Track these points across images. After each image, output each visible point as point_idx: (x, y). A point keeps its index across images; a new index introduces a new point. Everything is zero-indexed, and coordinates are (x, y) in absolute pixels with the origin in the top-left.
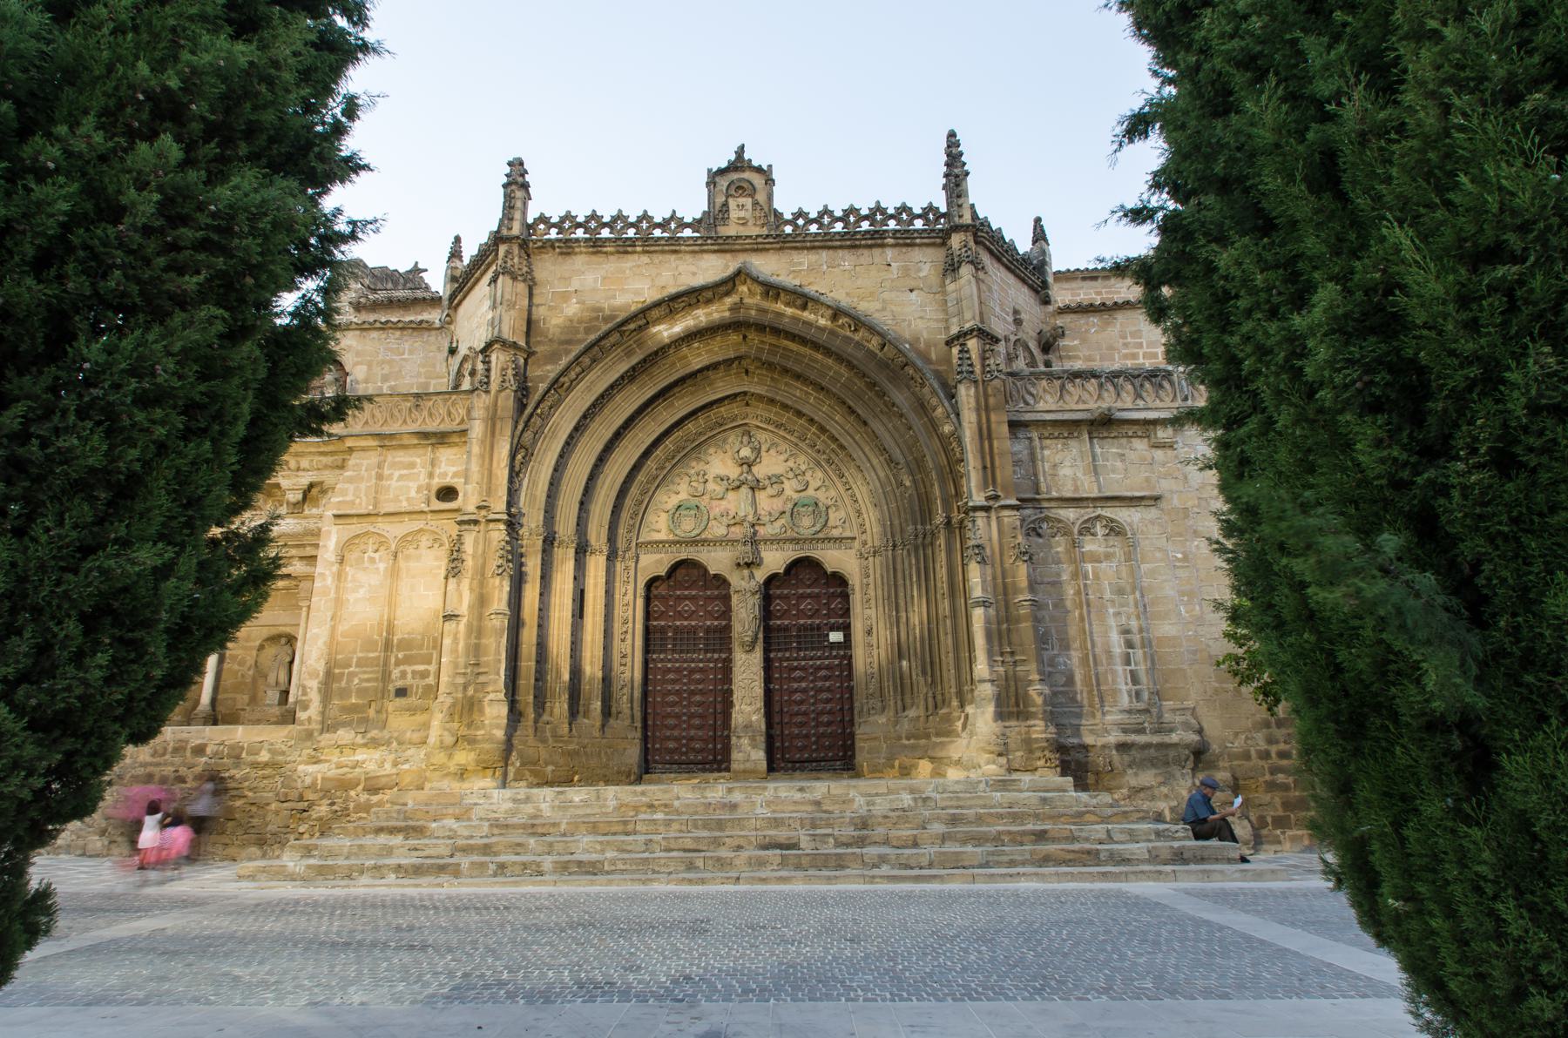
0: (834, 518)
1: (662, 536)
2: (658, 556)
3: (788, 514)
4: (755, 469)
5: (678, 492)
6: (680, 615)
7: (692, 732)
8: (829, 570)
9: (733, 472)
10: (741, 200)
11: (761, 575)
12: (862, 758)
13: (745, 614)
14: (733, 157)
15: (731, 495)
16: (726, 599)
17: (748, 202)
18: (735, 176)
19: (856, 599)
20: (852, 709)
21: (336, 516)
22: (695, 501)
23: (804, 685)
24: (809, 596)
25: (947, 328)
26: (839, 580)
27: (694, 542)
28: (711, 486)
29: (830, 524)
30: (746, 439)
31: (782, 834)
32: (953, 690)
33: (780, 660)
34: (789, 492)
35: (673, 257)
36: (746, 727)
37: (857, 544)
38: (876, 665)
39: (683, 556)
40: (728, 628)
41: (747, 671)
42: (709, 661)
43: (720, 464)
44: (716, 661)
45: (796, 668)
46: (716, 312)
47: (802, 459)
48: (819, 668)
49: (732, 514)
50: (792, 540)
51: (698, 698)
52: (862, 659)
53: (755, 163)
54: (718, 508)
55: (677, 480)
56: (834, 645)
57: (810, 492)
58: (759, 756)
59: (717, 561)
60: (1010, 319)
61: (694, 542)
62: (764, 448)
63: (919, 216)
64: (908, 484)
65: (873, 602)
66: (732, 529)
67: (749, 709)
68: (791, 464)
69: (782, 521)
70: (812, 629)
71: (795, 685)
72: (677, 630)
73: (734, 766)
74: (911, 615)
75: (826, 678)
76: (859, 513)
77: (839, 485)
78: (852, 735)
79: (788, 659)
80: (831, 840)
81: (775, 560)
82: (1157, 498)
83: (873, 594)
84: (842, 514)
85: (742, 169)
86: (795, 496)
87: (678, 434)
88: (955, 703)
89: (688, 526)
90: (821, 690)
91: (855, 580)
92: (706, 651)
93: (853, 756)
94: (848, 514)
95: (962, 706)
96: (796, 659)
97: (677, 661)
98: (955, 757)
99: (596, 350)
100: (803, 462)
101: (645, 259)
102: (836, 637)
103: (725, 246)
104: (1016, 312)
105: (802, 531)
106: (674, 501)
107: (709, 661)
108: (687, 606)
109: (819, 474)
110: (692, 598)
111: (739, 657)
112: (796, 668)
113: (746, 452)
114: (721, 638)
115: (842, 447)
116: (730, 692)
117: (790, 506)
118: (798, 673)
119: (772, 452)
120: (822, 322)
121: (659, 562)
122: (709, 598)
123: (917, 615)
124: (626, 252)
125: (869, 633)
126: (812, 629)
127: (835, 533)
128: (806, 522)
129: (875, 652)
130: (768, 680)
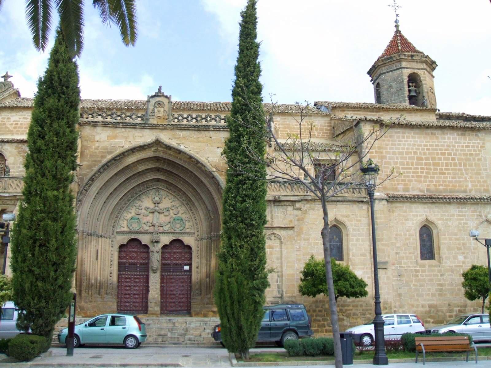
0: (188, 224)
1: (125, 229)
4: (160, 205)
5: (131, 213)
6: (131, 258)
8: (185, 244)
10: (160, 109)
11: (160, 246)
12: (192, 311)
13: (156, 259)
14: (157, 91)
15: (151, 215)
16: (148, 253)
17: (162, 109)
18: (158, 99)
22: (137, 216)
24: (178, 253)
27: (137, 232)
29: (187, 227)
31: (163, 332)
33: (167, 276)
34: (172, 214)
35: (133, 130)
38: (199, 279)
40: (147, 264)
41: (155, 281)
42: (141, 275)
43: (147, 202)
44: (143, 275)
45: (172, 279)
46: (148, 154)
49: (151, 222)
50: (172, 233)
51: (137, 288)
52: (195, 277)
53: (165, 94)
54: (145, 220)
55: (131, 208)
56: (186, 271)
57: (180, 215)
58: (158, 309)
59: (145, 239)
61: (137, 232)
62: (164, 197)
64: (212, 217)
69: (169, 226)
70: (178, 265)
72: (130, 264)
73: (149, 312)
76: (197, 224)
77: (191, 213)
78: (190, 302)
79: (169, 275)
81: (166, 240)
82: (293, 228)
84: (191, 224)
85: (160, 96)
89: (135, 226)
90: (180, 286)
91: (194, 248)
92: (140, 272)
93: (190, 310)
99: (106, 167)
100: (177, 203)
101: (123, 130)
102: (187, 268)
103: (153, 127)
105: (176, 229)
107: (141, 275)
109: (184, 208)
110: (135, 252)
112: (172, 279)
113: (157, 199)
114: (146, 267)
117: (172, 220)
118: (173, 280)
119: (167, 198)
121: (124, 239)
122: (141, 252)
124: (117, 127)
126: (178, 265)
127: (188, 231)
128: (178, 226)
129: (199, 274)
130: (162, 282)
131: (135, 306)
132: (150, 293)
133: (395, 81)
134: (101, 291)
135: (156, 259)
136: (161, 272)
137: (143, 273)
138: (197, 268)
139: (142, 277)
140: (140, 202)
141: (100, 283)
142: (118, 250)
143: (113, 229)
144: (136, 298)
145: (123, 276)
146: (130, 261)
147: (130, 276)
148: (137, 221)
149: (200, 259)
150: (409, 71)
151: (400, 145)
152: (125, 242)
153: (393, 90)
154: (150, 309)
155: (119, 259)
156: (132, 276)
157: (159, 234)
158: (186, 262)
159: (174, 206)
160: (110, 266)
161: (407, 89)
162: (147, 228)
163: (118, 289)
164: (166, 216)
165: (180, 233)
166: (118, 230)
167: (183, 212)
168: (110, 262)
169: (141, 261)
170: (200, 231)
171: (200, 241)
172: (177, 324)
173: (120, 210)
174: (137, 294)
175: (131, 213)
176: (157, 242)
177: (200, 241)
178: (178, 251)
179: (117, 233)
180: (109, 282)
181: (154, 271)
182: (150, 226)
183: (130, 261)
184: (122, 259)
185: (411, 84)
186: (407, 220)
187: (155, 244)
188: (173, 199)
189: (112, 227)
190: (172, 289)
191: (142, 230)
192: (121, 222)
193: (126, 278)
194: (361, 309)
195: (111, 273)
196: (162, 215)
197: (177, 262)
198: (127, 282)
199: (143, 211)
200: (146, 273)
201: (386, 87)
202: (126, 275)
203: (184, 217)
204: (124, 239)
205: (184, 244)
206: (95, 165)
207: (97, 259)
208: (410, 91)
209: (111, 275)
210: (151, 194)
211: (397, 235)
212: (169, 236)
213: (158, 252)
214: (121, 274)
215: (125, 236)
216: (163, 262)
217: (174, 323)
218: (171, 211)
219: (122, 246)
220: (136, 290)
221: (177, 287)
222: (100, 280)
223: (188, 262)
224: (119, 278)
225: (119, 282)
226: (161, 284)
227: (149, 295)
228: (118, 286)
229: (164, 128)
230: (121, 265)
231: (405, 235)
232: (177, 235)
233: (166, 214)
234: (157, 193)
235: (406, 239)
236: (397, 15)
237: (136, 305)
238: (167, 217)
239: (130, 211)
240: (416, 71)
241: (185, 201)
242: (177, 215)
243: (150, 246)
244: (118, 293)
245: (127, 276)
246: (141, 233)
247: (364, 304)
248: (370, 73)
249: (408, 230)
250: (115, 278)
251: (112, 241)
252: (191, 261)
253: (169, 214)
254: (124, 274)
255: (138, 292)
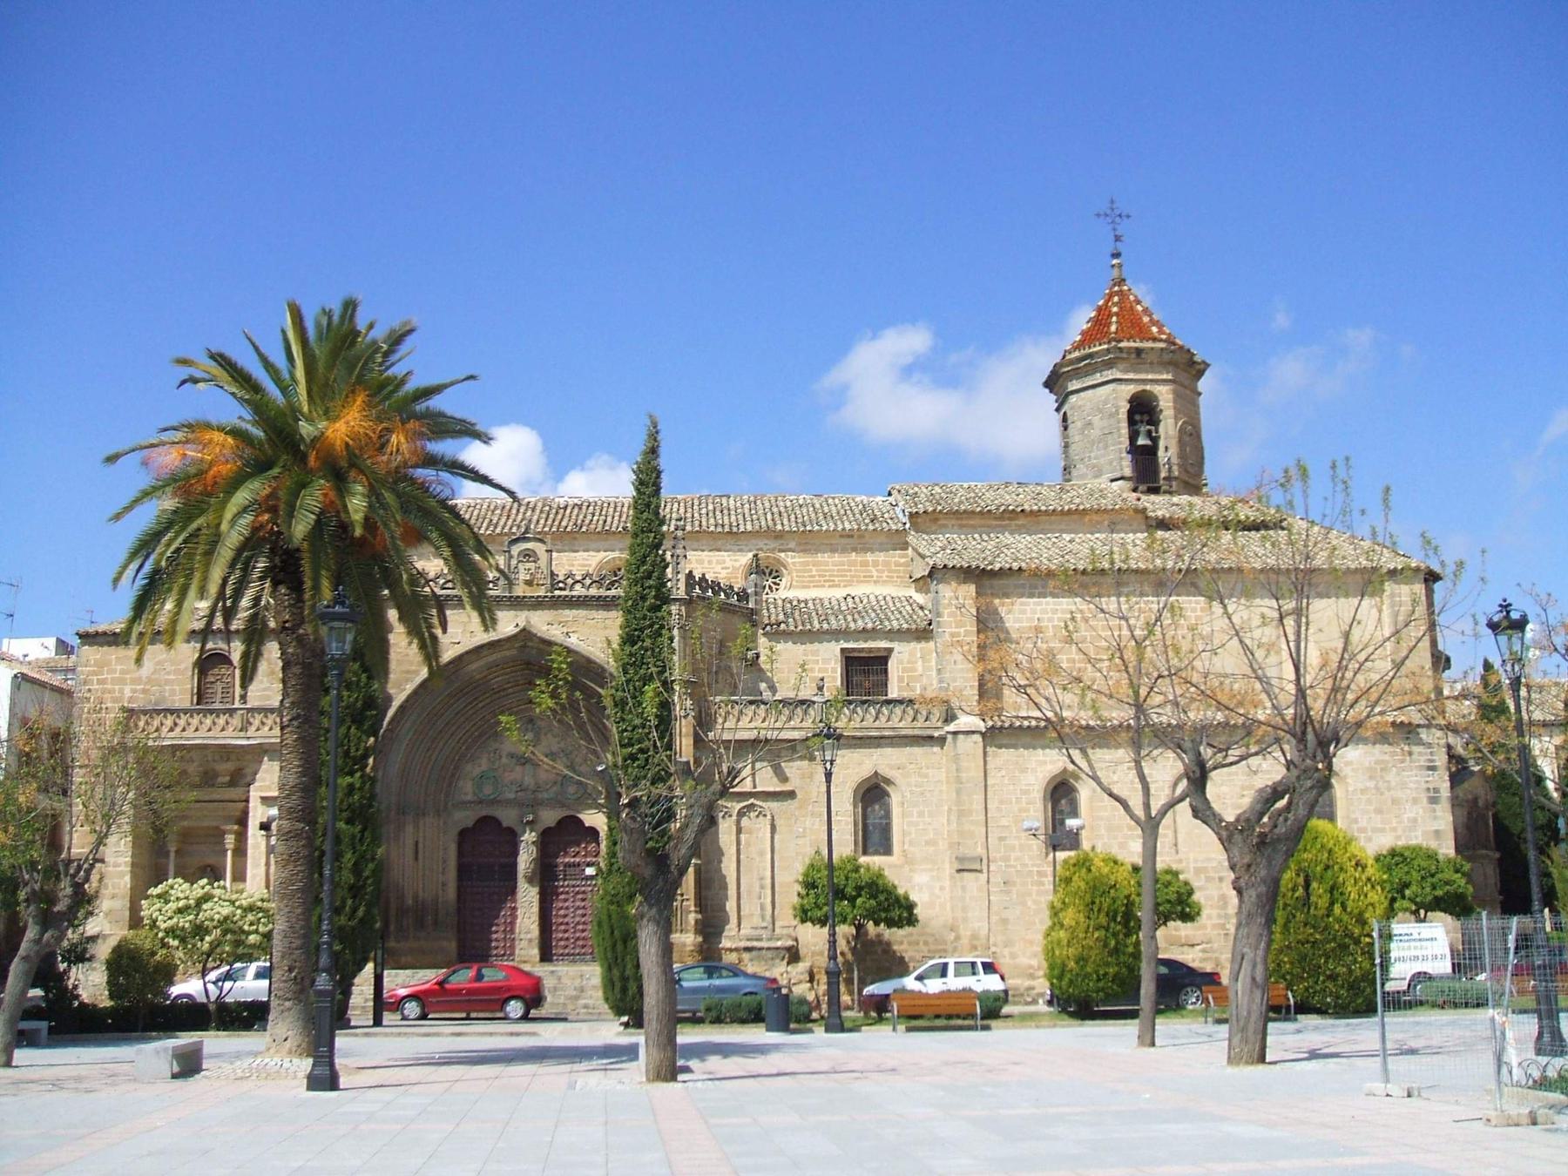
1: (469, 797)
15: (518, 768)
21: (263, 798)
28: (504, 760)
39: (484, 813)
59: (508, 817)
61: (494, 802)
89: (488, 790)
106: (477, 771)
133: (1100, 411)
150: (1131, 389)
151: (1024, 612)
152: (470, 823)
153: (1095, 433)
161: (1125, 431)
172: (564, 980)
185: (1137, 417)
186: (1024, 770)
192: (461, 783)
194: (925, 949)
201: (1079, 424)
204: (466, 818)
206: (407, 681)
207: (416, 858)
208: (1133, 437)
211: (1001, 802)
217: (559, 978)
219: (463, 834)
228: (459, 910)
229: (538, 604)
230: (463, 870)
231: (1018, 800)
235: (1020, 811)
236: (1118, 239)
240: (1148, 387)
247: (931, 940)
248: (1047, 384)
249: (1026, 792)
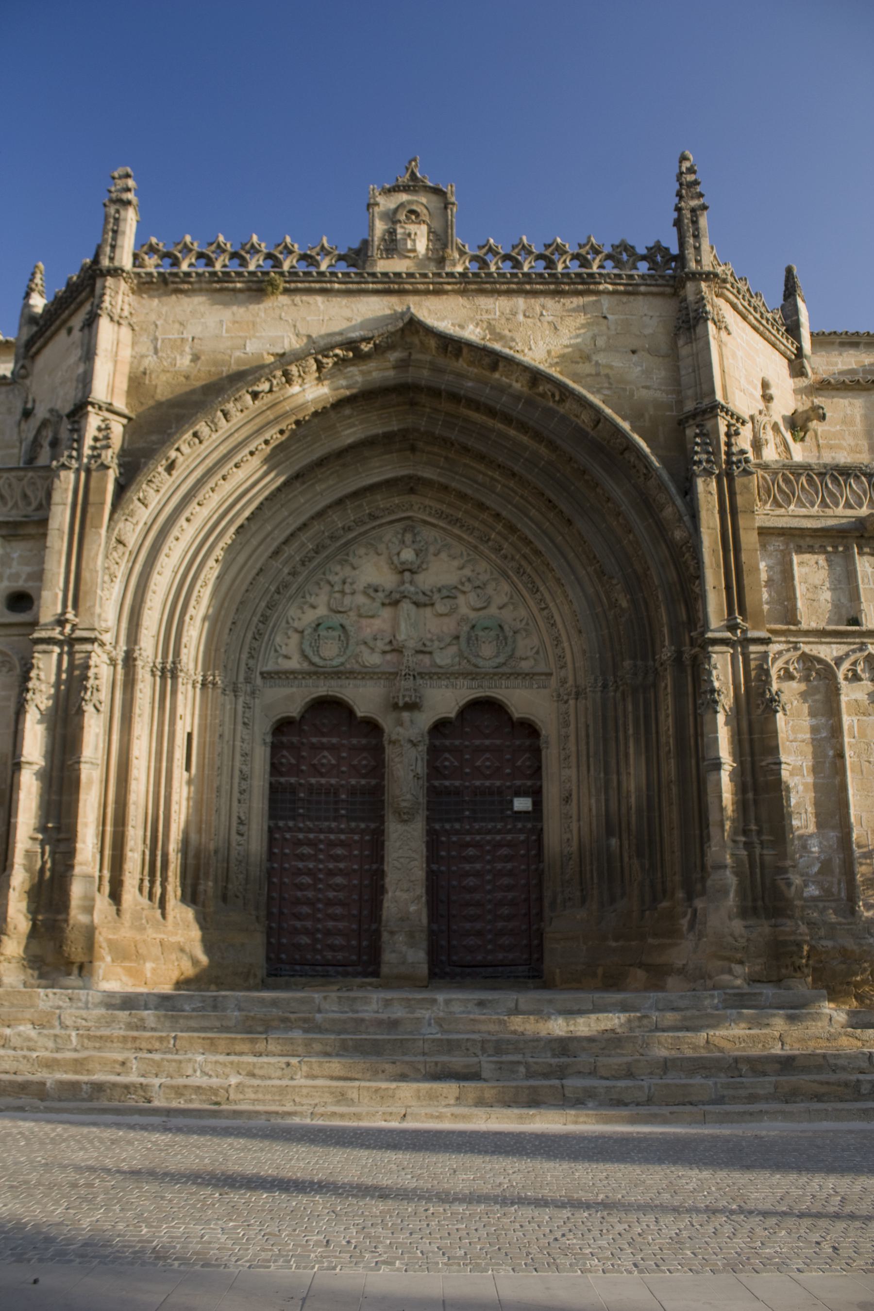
0: (525, 645)
1: (294, 664)
2: (287, 691)
3: (463, 640)
4: (420, 578)
6: (316, 770)
7: (330, 924)
8: (516, 715)
9: (387, 579)
13: (406, 771)
15: (386, 613)
16: (378, 751)
19: (551, 756)
20: (540, 899)
22: (338, 619)
23: (478, 866)
25: (680, 403)
26: (529, 729)
27: (337, 674)
29: (519, 653)
30: (408, 537)
32: (678, 878)
34: (464, 610)
35: (319, 299)
36: (402, 919)
37: (553, 681)
38: (575, 843)
41: (405, 850)
42: (352, 831)
43: (373, 571)
45: (468, 845)
47: (483, 566)
48: (499, 845)
50: (465, 675)
57: (493, 610)
58: (417, 957)
60: (759, 392)
61: (337, 674)
62: (432, 549)
63: (644, 258)
64: (625, 604)
65: (573, 759)
66: (389, 657)
67: (405, 896)
68: (467, 572)
71: (467, 867)
72: (311, 789)
73: (385, 970)
74: (624, 778)
75: (509, 858)
76: (557, 641)
77: (531, 603)
78: (540, 934)
79: (457, 832)
80: (522, 1069)
81: (445, 700)
83: (573, 749)
86: (473, 615)
87: (317, 527)
88: (680, 895)
89: (330, 651)
93: (541, 960)
94: (543, 642)
95: (690, 897)
96: (468, 832)
97: (310, 830)
98: (679, 963)
102: (522, 804)
104: (765, 385)
105: (481, 663)
106: (310, 616)
107: (352, 831)
108: (328, 758)
109: (506, 587)
110: (332, 748)
111: (394, 830)
112: (468, 845)
113: (408, 555)
114: (372, 802)
115: (537, 553)
116: (380, 874)
117: (466, 628)
118: (471, 851)
119: (443, 555)
120: (517, 386)
123: (634, 779)
125: (567, 800)
127: (525, 666)
128: (487, 650)
129: (574, 826)
131: (332, 948)
132: (390, 895)
134: (201, 888)
135: (406, 771)
136: (429, 819)
137: (363, 826)
138: (567, 800)
139: (356, 837)
140: (348, 569)
141: (197, 856)
142: (269, 739)
143: (251, 662)
144: (334, 918)
145: (288, 836)
146: (313, 781)
147: (311, 836)
148: (336, 634)
149: (574, 770)
152: (294, 711)
154: (388, 957)
155: (272, 774)
156: (322, 836)
157: (420, 681)
158: (518, 783)
159: (469, 580)
160: (236, 795)
162: (373, 659)
163: (270, 883)
164: (441, 615)
165: (495, 674)
166: (265, 669)
167: (505, 599)
168: (236, 780)
169: (353, 782)
170: (570, 665)
171: (572, 702)
173: (276, 597)
174: (341, 903)
175: (314, 607)
176: (413, 707)
177: (572, 702)
178: (487, 742)
179: (266, 676)
180: (234, 854)
181: (405, 817)
182: (384, 652)
183: (313, 781)
184: (282, 774)
187: (406, 715)
188: (465, 558)
189: (244, 656)
190: (471, 881)
191: (356, 667)
193: (299, 843)
195: (241, 822)
196: (428, 611)
197: (487, 783)
198: (302, 857)
199: (361, 599)
200: (373, 826)
202: (300, 830)
203: (507, 615)
204: (292, 700)
205: (510, 718)
209: (243, 829)
210: (386, 539)
212: (454, 686)
213: (415, 745)
214: (279, 828)
215: (294, 689)
216: (436, 783)
218: (461, 599)
219: (283, 726)
220: (337, 888)
221: (489, 877)
222: (200, 844)
223: (529, 783)
224: (271, 841)
225: (271, 854)
226: (428, 865)
227: (386, 904)
228: (270, 872)
232: (486, 683)
233: (440, 608)
234: (408, 537)
237: (339, 941)
238: (446, 620)
239: (312, 600)
241: (513, 558)
242: (481, 613)
243: (380, 720)
244: (270, 898)
245: (301, 836)
246: (351, 674)
250: (256, 842)
251: (247, 706)
252: (540, 778)
253: (454, 610)
254: (290, 829)
255: (341, 895)
